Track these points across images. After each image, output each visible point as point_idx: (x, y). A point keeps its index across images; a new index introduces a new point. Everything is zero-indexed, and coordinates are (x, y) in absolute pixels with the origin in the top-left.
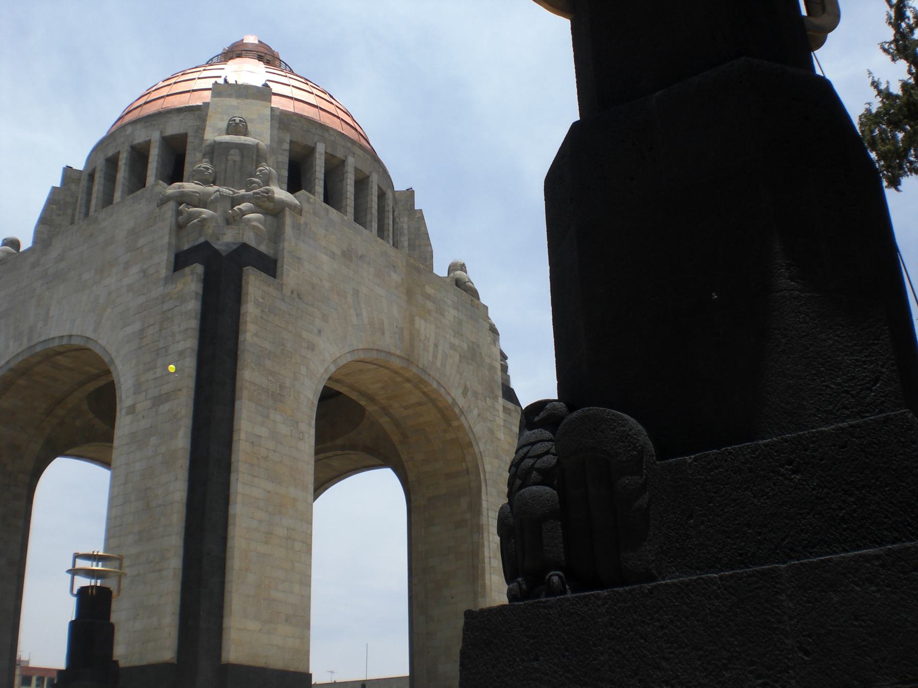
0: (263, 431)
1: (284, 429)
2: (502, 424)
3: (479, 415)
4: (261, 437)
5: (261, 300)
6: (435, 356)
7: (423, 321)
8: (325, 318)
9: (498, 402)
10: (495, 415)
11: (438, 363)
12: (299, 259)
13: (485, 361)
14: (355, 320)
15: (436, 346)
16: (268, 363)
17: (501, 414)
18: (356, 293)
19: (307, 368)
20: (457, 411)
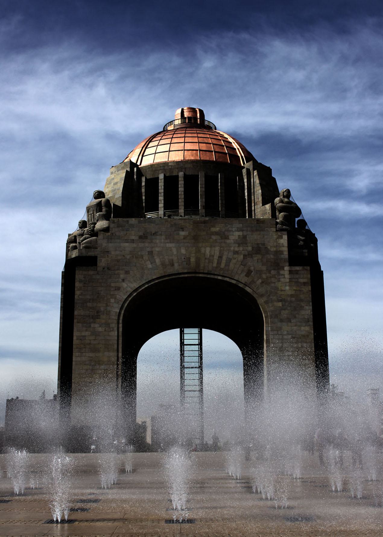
0: (87, 333)
1: (100, 329)
2: (288, 280)
3: (262, 282)
4: (85, 336)
5: (84, 279)
6: (219, 263)
7: (208, 250)
8: (127, 272)
9: (284, 270)
10: (279, 278)
11: (223, 265)
12: (108, 252)
13: (270, 251)
14: (150, 266)
15: (220, 257)
16: (89, 305)
17: (287, 276)
18: (151, 253)
19: (115, 299)
20: (241, 285)
